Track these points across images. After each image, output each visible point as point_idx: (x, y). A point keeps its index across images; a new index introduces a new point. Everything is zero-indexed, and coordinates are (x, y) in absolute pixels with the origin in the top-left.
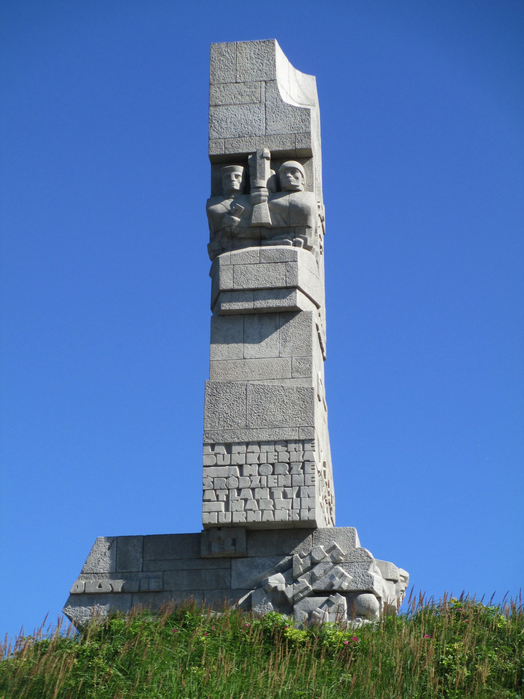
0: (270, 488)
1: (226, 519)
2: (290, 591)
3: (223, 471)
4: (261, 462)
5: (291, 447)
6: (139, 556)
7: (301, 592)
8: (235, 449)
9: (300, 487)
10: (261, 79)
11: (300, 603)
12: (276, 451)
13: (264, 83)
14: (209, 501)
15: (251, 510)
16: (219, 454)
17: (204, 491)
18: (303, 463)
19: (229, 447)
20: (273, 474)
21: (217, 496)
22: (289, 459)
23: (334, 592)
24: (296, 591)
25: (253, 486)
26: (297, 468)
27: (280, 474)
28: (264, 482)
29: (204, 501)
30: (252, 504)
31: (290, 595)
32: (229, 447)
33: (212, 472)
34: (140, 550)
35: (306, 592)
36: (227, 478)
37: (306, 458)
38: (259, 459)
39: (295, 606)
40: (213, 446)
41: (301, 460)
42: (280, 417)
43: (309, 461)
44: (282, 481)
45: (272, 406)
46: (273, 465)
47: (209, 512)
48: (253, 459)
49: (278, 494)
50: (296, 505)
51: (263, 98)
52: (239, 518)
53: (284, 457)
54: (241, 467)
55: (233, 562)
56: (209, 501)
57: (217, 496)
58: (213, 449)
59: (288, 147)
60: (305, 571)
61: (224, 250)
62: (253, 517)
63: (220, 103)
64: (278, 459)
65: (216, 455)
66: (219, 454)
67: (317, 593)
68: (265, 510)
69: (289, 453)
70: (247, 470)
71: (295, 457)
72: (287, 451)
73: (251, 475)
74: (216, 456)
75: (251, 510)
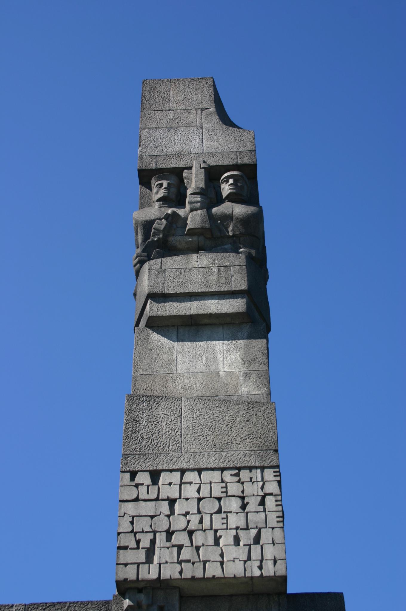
0: (216, 531)
3: (148, 508)
4: (201, 496)
5: (245, 475)
8: (164, 478)
9: (260, 529)
10: (198, 107)
12: (223, 481)
13: (199, 111)
15: (188, 561)
16: (142, 484)
19: (155, 476)
20: (219, 511)
21: (138, 542)
22: (243, 492)
27: (231, 512)
32: (155, 476)
33: (130, 509)
36: (152, 517)
38: (198, 491)
44: (235, 521)
46: (219, 499)
48: (190, 491)
54: (172, 502)
56: (126, 548)
57: (138, 542)
58: (132, 478)
59: (228, 161)
64: (226, 492)
65: (137, 486)
66: (142, 484)
68: (209, 561)
72: (239, 481)
74: (137, 488)
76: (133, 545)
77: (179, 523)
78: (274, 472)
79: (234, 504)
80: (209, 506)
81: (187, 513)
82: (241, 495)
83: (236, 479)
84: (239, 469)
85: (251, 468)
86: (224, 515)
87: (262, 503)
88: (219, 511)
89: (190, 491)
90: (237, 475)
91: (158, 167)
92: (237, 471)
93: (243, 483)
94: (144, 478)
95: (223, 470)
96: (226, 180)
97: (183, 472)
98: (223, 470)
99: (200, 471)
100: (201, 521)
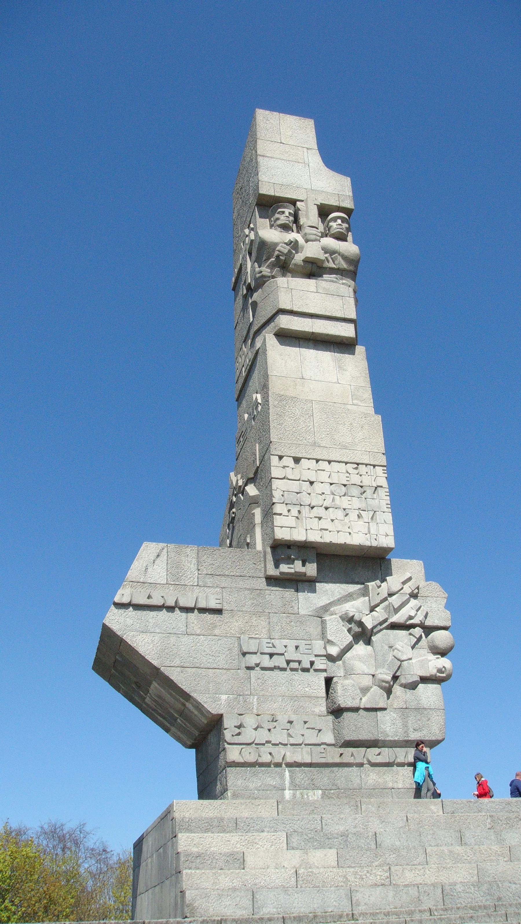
0: (344, 509)
1: (299, 536)
2: (369, 622)
3: (294, 486)
5: (363, 469)
6: (193, 567)
7: (381, 624)
9: (375, 512)
11: (379, 635)
14: (280, 514)
16: (288, 467)
17: (274, 504)
18: (376, 488)
19: (297, 460)
21: (289, 511)
23: (413, 626)
24: (376, 623)
25: (326, 504)
26: (369, 492)
27: (354, 497)
29: (275, 514)
31: (369, 626)
32: (297, 460)
34: (194, 561)
35: (384, 625)
36: (298, 493)
39: (374, 638)
40: (281, 458)
42: (349, 440)
43: (381, 487)
45: (341, 427)
47: (282, 527)
49: (353, 515)
50: (373, 531)
51: (306, 160)
52: (314, 537)
53: (355, 479)
54: (312, 483)
55: (300, 585)
56: (280, 514)
57: (289, 511)
60: (383, 601)
61: (273, 277)
62: (328, 538)
63: (268, 155)
67: (394, 626)
69: (361, 475)
70: (318, 488)
71: (367, 481)
73: (323, 493)
75: (327, 530)
76: (285, 512)
78: (383, 470)
81: (323, 493)
82: (361, 484)
83: (356, 472)
84: (358, 464)
85: (366, 465)
86: (349, 498)
89: (323, 476)
90: (356, 468)
91: (277, 195)
92: (356, 466)
93: (361, 475)
94: (288, 462)
95: (346, 463)
96: (335, 219)
97: (317, 461)
98: (346, 463)
99: (330, 462)
100: (333, 500)
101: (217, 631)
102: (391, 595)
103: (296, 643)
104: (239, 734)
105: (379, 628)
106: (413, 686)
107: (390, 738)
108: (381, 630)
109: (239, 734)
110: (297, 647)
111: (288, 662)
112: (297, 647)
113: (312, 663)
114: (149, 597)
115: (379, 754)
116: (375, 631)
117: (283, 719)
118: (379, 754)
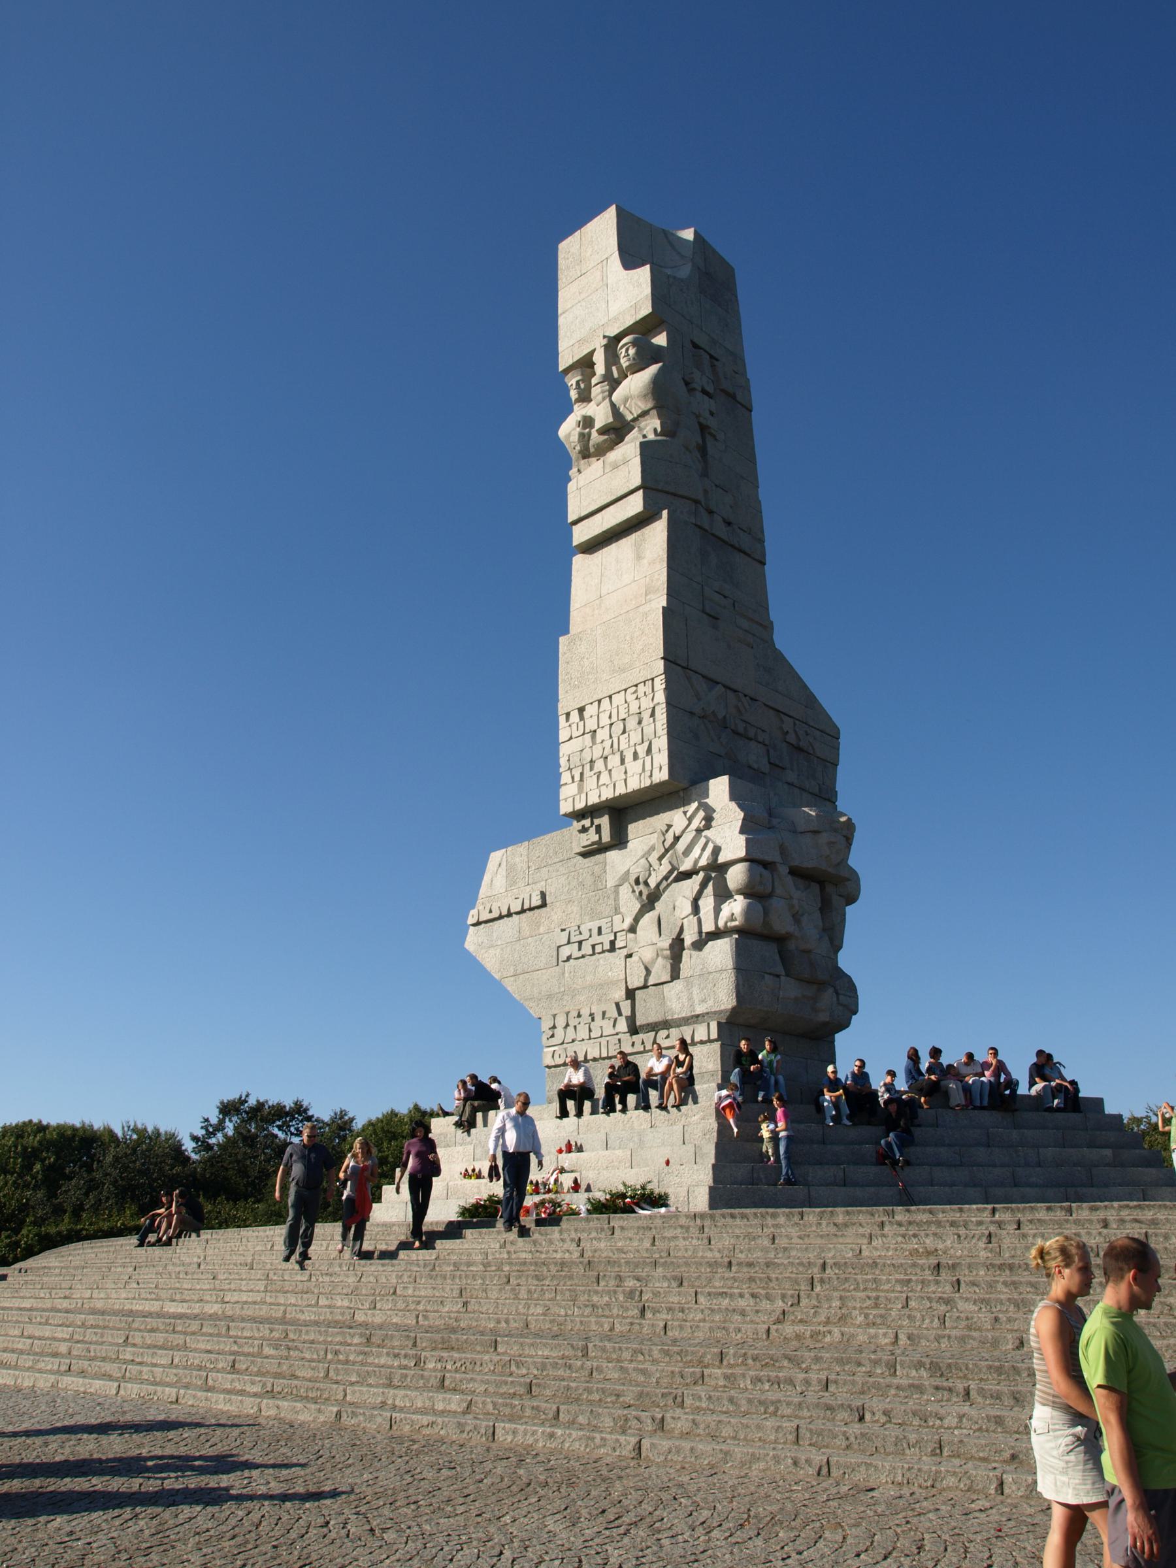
7: (666, 878)
8: (590, 711)
19: (581, 710)
21: (573, 778)
28: (615, 746)
30: (604, 778)
37: (656, 701)
38: (610, 717)
41: (652, 705)
48: (605, 721)
50: (648, 767)
52: (594, 799)
70: (602, 734)
77: (597, 752)
79: (632, 723)
80: (618, 728)
87: (653, 714)
88: (624, 732)
101: (542, 930)
102: (677, 839)
103: (596, 924)
104: (552, 1036)
105: (665, 883)
106: (699, 945)
107: (676, 1016)
108: (668, 885)
109: (552, 1036)
110: (600, 929)
111: (593, 947)
112: (600, 929)
113: (612, 943)
114: (491, 911)
115: (668, 1037)
116: (661, 888)
117: (585, 1012)
118: (668, 1037)
